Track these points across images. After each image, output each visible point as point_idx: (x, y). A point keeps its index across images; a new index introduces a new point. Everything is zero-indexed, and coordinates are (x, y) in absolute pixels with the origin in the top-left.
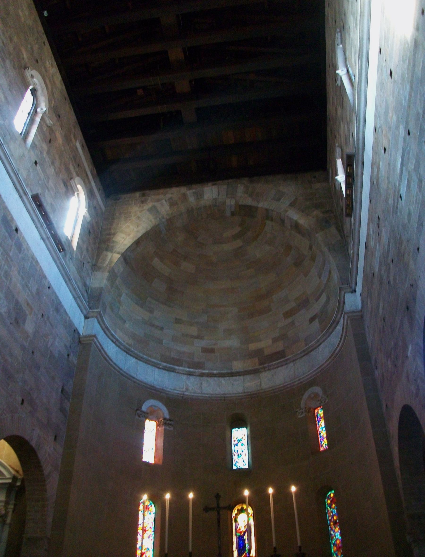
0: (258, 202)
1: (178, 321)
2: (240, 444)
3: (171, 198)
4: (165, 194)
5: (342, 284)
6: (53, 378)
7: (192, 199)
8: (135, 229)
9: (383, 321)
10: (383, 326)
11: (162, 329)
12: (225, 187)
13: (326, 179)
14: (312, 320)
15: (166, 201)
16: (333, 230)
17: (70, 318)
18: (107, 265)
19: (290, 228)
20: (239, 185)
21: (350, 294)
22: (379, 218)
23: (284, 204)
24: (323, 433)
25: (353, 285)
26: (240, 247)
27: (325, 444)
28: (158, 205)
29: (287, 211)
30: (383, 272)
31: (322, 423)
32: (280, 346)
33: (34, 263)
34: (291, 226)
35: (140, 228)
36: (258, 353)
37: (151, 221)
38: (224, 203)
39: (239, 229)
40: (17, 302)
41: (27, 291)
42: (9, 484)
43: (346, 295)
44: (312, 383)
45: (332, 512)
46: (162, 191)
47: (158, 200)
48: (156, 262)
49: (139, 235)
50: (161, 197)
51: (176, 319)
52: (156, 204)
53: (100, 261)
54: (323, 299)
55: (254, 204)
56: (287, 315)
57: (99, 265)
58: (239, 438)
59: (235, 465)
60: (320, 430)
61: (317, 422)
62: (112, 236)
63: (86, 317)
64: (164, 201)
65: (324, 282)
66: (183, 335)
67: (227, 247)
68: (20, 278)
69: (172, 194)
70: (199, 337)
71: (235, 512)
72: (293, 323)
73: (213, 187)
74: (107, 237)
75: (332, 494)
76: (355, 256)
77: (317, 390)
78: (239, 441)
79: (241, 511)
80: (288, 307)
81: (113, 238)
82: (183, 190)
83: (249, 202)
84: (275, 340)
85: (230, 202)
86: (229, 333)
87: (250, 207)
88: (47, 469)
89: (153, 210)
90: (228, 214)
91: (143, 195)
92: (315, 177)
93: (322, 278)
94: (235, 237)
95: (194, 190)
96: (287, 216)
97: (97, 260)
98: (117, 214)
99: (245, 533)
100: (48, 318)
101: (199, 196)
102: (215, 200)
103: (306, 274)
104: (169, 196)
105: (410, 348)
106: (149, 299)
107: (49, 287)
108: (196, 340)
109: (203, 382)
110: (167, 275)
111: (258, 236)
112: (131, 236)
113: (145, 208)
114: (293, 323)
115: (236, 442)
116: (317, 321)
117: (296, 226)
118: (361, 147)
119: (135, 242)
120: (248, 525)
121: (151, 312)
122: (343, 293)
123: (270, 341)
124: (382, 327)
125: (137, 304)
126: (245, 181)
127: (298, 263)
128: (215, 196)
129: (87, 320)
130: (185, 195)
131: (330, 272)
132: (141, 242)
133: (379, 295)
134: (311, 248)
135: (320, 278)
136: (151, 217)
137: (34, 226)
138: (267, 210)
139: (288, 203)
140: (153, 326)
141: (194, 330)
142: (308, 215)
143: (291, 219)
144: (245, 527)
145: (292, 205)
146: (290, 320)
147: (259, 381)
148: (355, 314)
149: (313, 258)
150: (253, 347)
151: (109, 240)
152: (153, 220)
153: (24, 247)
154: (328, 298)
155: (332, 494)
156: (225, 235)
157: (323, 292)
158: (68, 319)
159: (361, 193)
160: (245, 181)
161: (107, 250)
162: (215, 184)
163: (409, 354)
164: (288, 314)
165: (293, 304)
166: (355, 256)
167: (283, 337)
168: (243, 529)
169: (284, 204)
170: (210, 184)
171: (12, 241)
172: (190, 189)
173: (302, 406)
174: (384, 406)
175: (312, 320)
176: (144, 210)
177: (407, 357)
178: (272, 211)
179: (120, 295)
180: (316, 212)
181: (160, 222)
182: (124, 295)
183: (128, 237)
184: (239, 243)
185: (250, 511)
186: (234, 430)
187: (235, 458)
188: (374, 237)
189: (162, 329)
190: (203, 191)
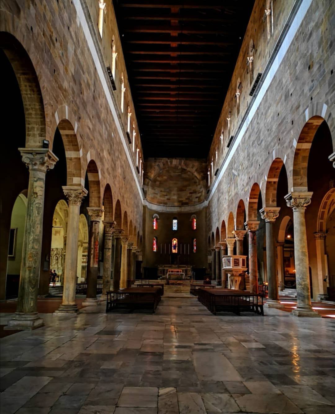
1: (161, 191)
7: (169, 164)
14: (196, 197)
16: (205, 181)
23: (194, 169)
24: (195, 225)
27: (195, 228)
28: (159, 163)
29: (194, 172)
31: (195, 223)
32: (187, 201)
38: (178, 167)
44: (194, 213)
47: (160, 162)
49: (155, 174)
54: (200, 194)
56: (191, 193)
63: (144, 199)
70: (166, 195)
71: (173, 240)
72: (191, 196)
75: (195, 239)
77: (195, 216)
79: (175, 240)
82: (167, 159)
83: (185, 167)
84: (186, 199)
85: (180, 167)
86: (174, 194)
89: (158, 165)
94: (179, 172)
101: (171, 162)
102: (176, 165)
104: (163, 161)
114: (191, 196)
116: (197, 199)
117: (196, 177)
120: (176, 243)
121: (155, 190)
123: (185, 199)
130: (167, 162)
141: (165, 194)
145: (196, 170)
146: (191, 195)
150: (180, 199)
155: (195, 239)
162: (175, 159)
164: (191, 193)
165: (192, 191)
167: (188, 199)
172: (169, 159)
173: (191, 218)
175: (196, 197)
180: (202, 174)
181: (161, 171)
184: (180, 173)
185: (177, 240)
187: (174, 227)
190: (172, 161)
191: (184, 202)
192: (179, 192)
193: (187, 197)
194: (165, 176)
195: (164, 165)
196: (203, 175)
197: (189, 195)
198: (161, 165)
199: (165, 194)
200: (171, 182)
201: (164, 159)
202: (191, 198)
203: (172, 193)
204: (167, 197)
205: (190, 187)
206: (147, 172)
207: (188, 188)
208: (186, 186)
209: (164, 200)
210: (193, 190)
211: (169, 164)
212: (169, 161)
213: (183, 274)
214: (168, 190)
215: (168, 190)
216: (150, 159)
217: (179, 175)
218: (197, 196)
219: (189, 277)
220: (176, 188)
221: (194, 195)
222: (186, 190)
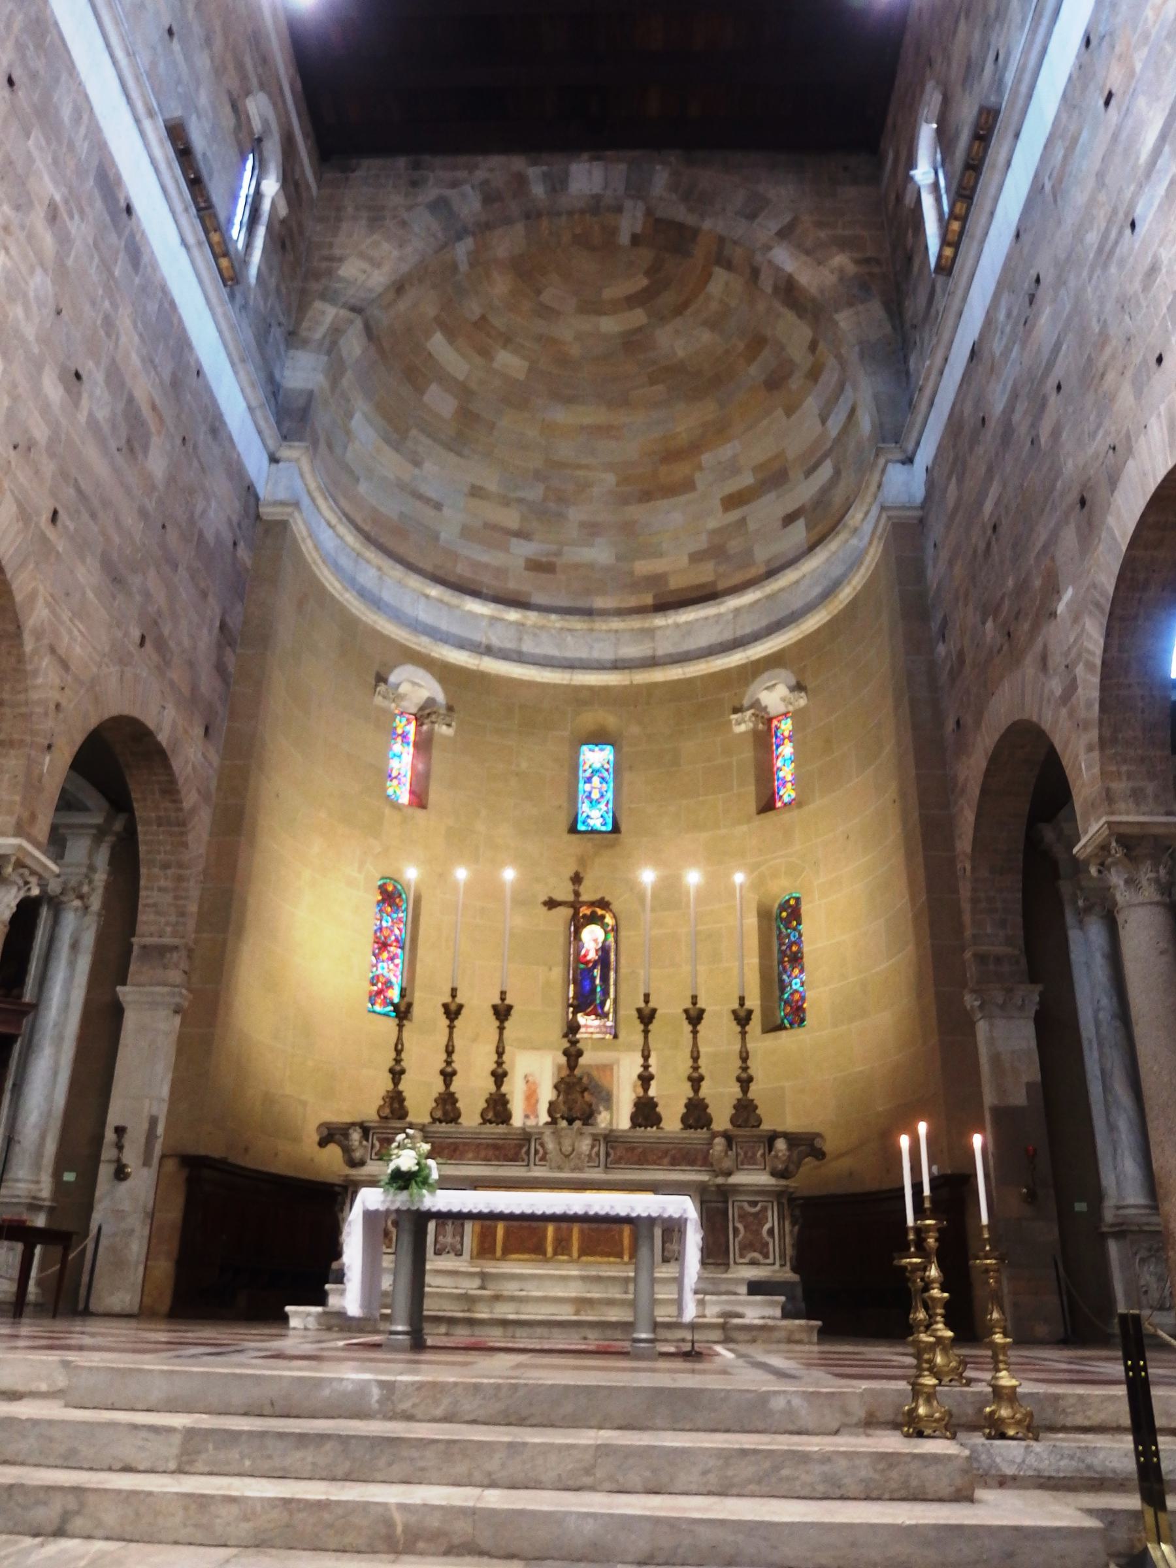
0: (702, 216)
1: (476, 492)
2: (596, 780)
3: (486, 182)
4: (472, 169)
5: (884, 441)
6: (204, 595)
7: (538, 190)
8: (396, 253)
9: (989, 532)
10: (989, 545)
11: (438, 506)
12: (623, 167)
13: (874, 179)
14: (789, 519)
15: (473, 187)
17: (239, 455)
18: (324, 337)
19: (769, 290)
20: (658, 167)
21: (899, 466)
22: (1038, 280)
25: (910, 446)
26: (640, 330)
30: (1017, 417)
31: (787, 750)
32: (705, 573)
33: (166, 306)
34: (776, 288)
35: (408, 250)
36: (656, 580)
37: (434, 236)
39: (645, 282)
40: (131, 400)
41: (153, 373)
42: (98, 827)
43: (890, 467)
45: (788, 936)
46: (463, 159)
47: (454, 184)
48: (438, 343)
49: (405, 268)
50: (461, 174)
51: (473, 487)
52: (448, 192)
53: (305, 324)
54: (826, 471)
55: (690, 219)
57: (304, 333)
58: (597, 766)
59: (584, 822)
60: (779, 763)
61: (774, 747)
62: (335, 265)
63: (274, 460)
64: (467, 188)
65: (834, 433)
66: (487, 526)
67: (610, 325)
68: (136, 338)
69: (491, 170)
72: (743, 521)
73: (595, 163)
74: (324, 265)
76: (933, 377)
78: (594, 772)
80: (733, 486)
81: (339, 268)
82: (518, 163)
83: (681, 213)
84: (696, 558)
86: (592, 530)
87: (681, 227)
88: (190, 798)
89: (440, 206)
90: (624, 239)
91: (416, 166)
92: (846, 169)
93: (830, 423)
94: (632, 301)
95: (545, 168)
96: (770, 262)
97: (299, 322)
98: (350, 210)
99: (595, 963)
100: (195, 447)
101: (558, 184)
103: (790, 411)
104: (480, 175)
105: (1068, 594)
106: (414, 432)
107: (198, 373)
108: (514, 540)
109: (525, 637)
110: (461, 378)
111: (685, 305)
112: (386, 268)
113: (420, 199)
114: (743, 521)
115: (588, 774)
116: (801, 523)
118: (1024, 89)
119: (394, 283)
121: (417, 464)
122: (882, 461)
123: (685, 560)
124: (982, 546)
125: (387, 441)
126: (672, 159)
127: (774, 382)
128: (597, 189)
129: (274, 466)
130: (521, 181)
131: (853, 411)
132: (407, 287)
133: (990, 470)
134: (813, 347)
135: (824, 421)
136: (435, 226)
137: (166, 208)
138: (721, 240)
139: (774, 226)
140: (420, 497)
141: (511, 518)
142: (819, 264)
143: (778, 269)
144: (597, 951)
146: (734, 515)
147: (651, 645)
148: (908, 513)
149: (814, 374)
150: (643, 567)
151: (330, 273)
152: (439, 235)
153: (145, 259)
154: (837, 473)
156: (609, 293)
157: (826, 455)
158: (236, 456)
159: (992, 214)
160: (672, 159)
161: (323, 297)
162: (598, 159)
163: (1061, 608)
164: (732, 501)
165: (747, 479)
166: (935, 372)
167: (715, 552)
168: (592, 956)
169: (767, 227)
170: (585, 156)
171: (120, 235)
172: (534, 163)
174: (950, 725)
175: (789, 519)
176: (417, 205)
177: (1053, 615)
178: (735, 243)
179: (349, 415)
182: (358, 416)
183: (376, 272)
184: (638, 317)
186: (585, 748)
188: (1008, 329)
189: (438, 506)
191: (675, 583)
192: (636, 512)
193: (702, 543)
194: (507, 340)
195: (490, 198)
196: (851, 269)
197: (717, 520)
198: (469, 205)
199: (511, 518)
200: (561, 415)
201: (496, 160)
202: (734, 545)
203: (576, 514)
204: (523, 550)
205: (726, 451)
206: (337, 252)
207: (707, 458)
208: (694, 448)
209: (500, 572)
210: (756, 469)
211: (538, 190)
212: (533, 173)
213: (673, 1229)
214: (535, 493)
215: (535, 493)
216: (368, 167)
217: (633, 342)
218: (791, 507)
219: (755, 1288)
220: (610, 479)
221: (770, 507)
222: (688, 485)
